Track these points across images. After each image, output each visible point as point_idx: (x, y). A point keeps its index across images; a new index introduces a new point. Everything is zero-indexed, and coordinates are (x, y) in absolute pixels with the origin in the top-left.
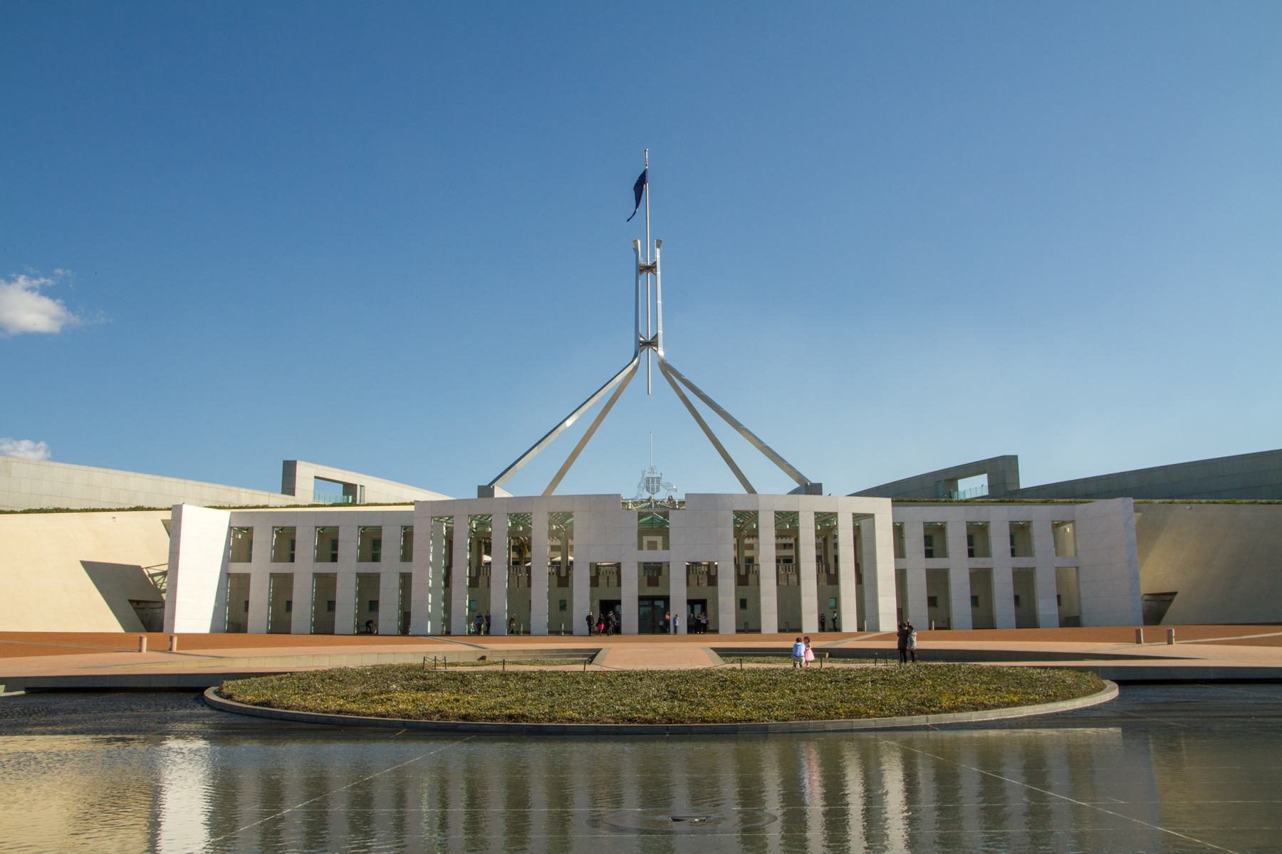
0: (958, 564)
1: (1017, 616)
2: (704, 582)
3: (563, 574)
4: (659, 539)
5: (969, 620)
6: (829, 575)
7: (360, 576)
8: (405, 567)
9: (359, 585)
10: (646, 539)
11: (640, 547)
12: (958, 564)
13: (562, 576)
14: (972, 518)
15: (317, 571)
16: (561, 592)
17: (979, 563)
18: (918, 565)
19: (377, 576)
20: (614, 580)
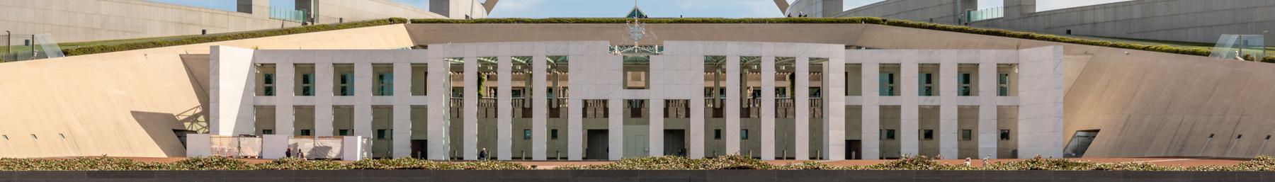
0: (910, 100)
1: (960, 149)
2: (683, 114)
3: (554, 106)
4: (643, 74)
5: (956, 151)
6: (785, 111)
7: (375, 108)
8: (419, 100)
9: (296, 115)
10: (629, 73)
11: (625, 86)
12: (910, 100)
13: (555, 111)
14: (924, 60)
15: (298, 104)
16: (556, 123)
17: (928, 101)
18: (871, 100)
19: (390, 108)
20: (601, 112)
